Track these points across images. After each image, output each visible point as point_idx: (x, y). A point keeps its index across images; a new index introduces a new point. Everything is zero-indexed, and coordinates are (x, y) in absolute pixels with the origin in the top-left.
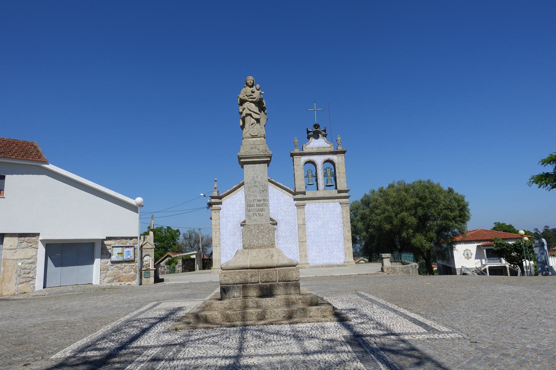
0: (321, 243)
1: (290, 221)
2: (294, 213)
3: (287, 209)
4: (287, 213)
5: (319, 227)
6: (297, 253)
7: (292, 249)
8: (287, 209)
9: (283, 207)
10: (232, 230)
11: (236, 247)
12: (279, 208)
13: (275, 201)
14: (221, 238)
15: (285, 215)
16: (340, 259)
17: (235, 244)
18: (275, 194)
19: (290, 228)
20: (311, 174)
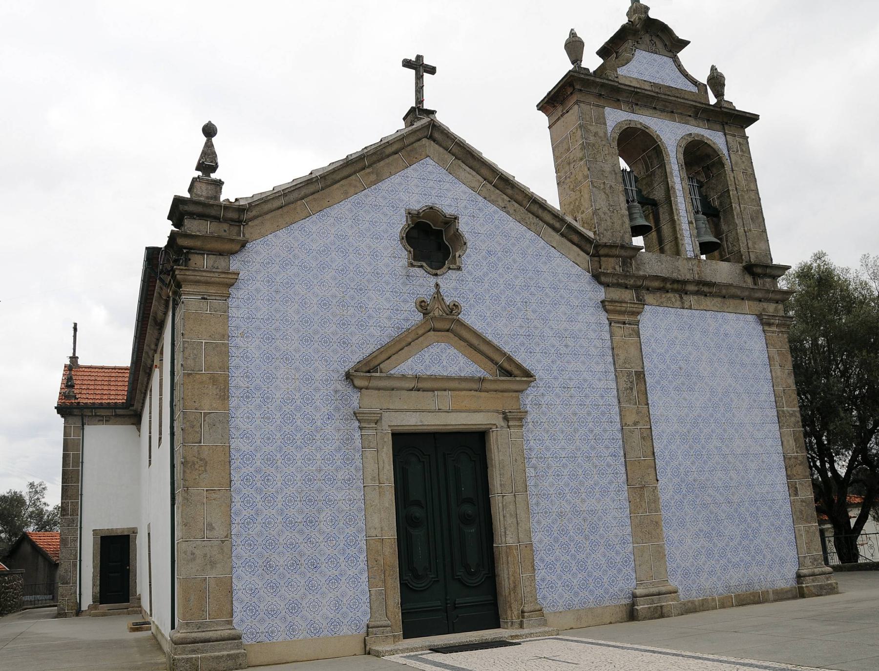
0: (710, 491)
1: (585, 380)
2: (598, 343)
3: (570, 320)
4: (570, 343)
5: (700, 416)
6: (624, 542)
7: (600, 519)
8: (570, 320)
9: (549, 312)
10: (298, 409)
11: (319, 511)
12: (534, 311)
13: (516, 277)
14: (238, 450)
15: (563, 350)
16: (782, 561)
17: (320, 490)
18: (514, 245)
19: (589, 414)
20: (634, 188)
